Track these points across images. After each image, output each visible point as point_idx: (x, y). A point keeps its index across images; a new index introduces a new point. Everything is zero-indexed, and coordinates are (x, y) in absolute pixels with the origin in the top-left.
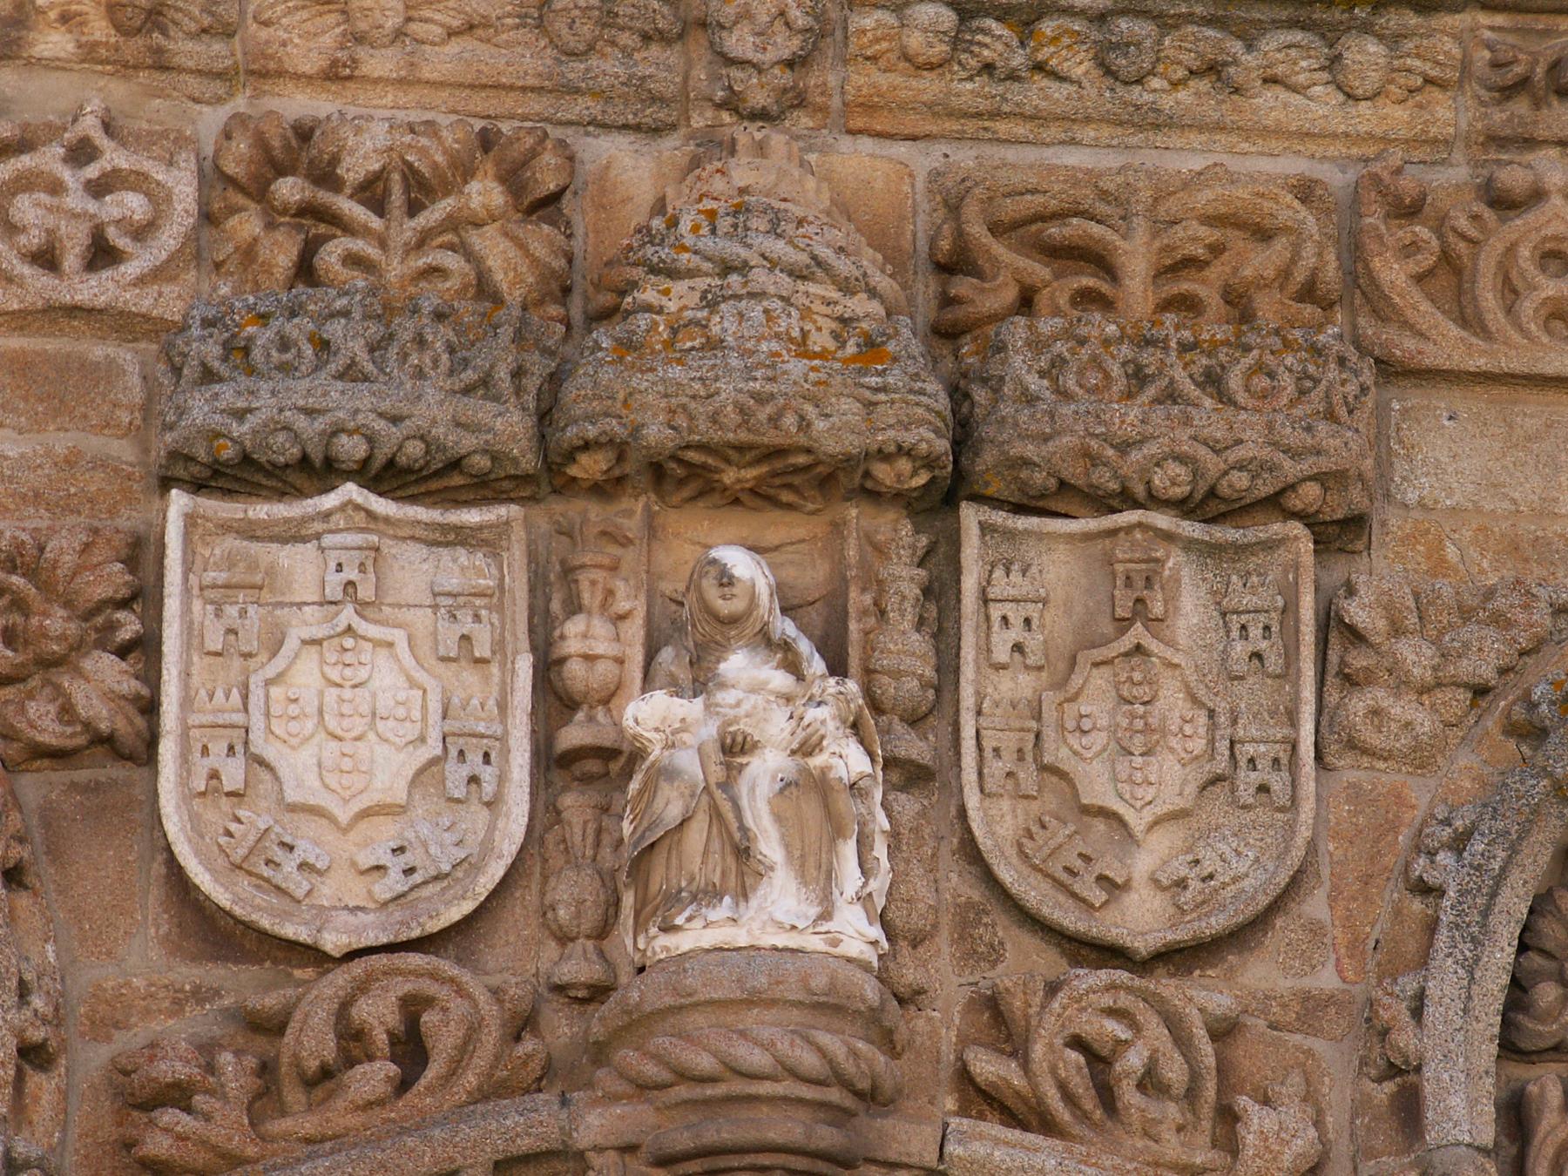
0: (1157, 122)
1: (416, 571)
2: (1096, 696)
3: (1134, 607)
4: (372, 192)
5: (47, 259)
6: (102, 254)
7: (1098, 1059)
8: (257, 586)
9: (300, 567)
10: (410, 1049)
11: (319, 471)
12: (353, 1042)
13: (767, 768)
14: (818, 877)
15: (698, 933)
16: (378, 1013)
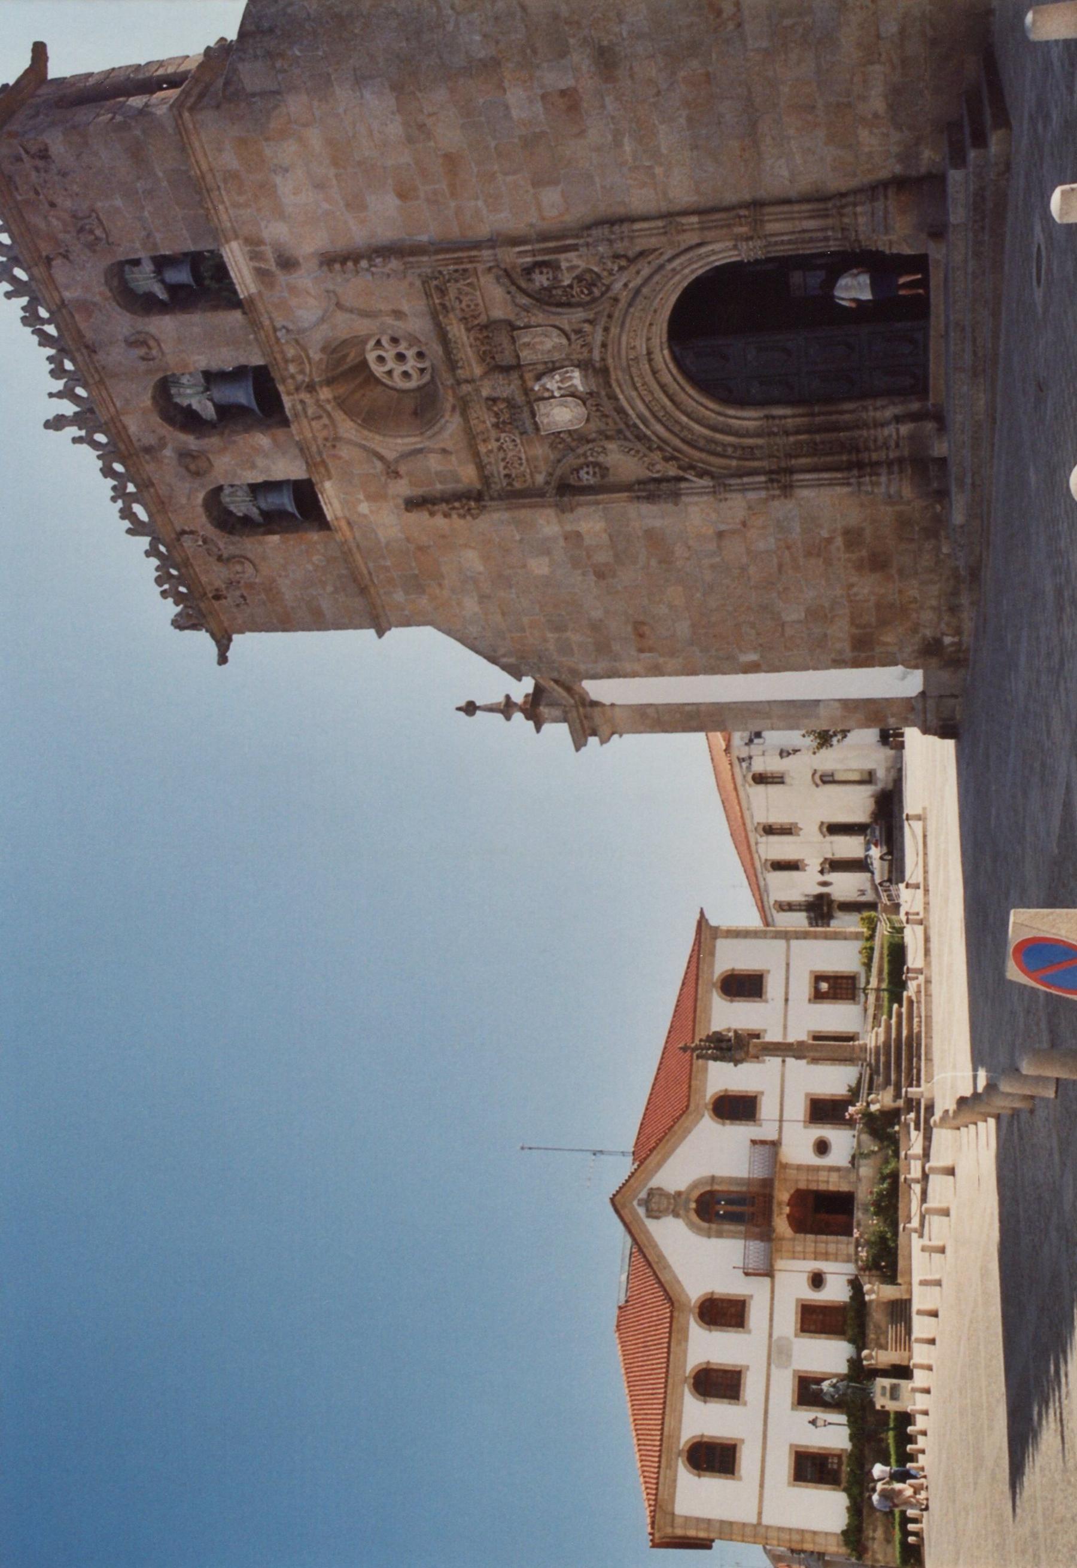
0: (463, 345)
1: (543, 411)
2: (539, 347)
3: (527, 345)
4: (498, 418)
5: (516, 445)
6: (514, 441)
7: (582, 346)
8: (548, 424)
9: (546, 421)
10: (597, 405)
11: (535, 423)
12: (597, 410)
13: (560, 384)
14: (571, 378)
15: (581, 388)
16: (594, 409)
